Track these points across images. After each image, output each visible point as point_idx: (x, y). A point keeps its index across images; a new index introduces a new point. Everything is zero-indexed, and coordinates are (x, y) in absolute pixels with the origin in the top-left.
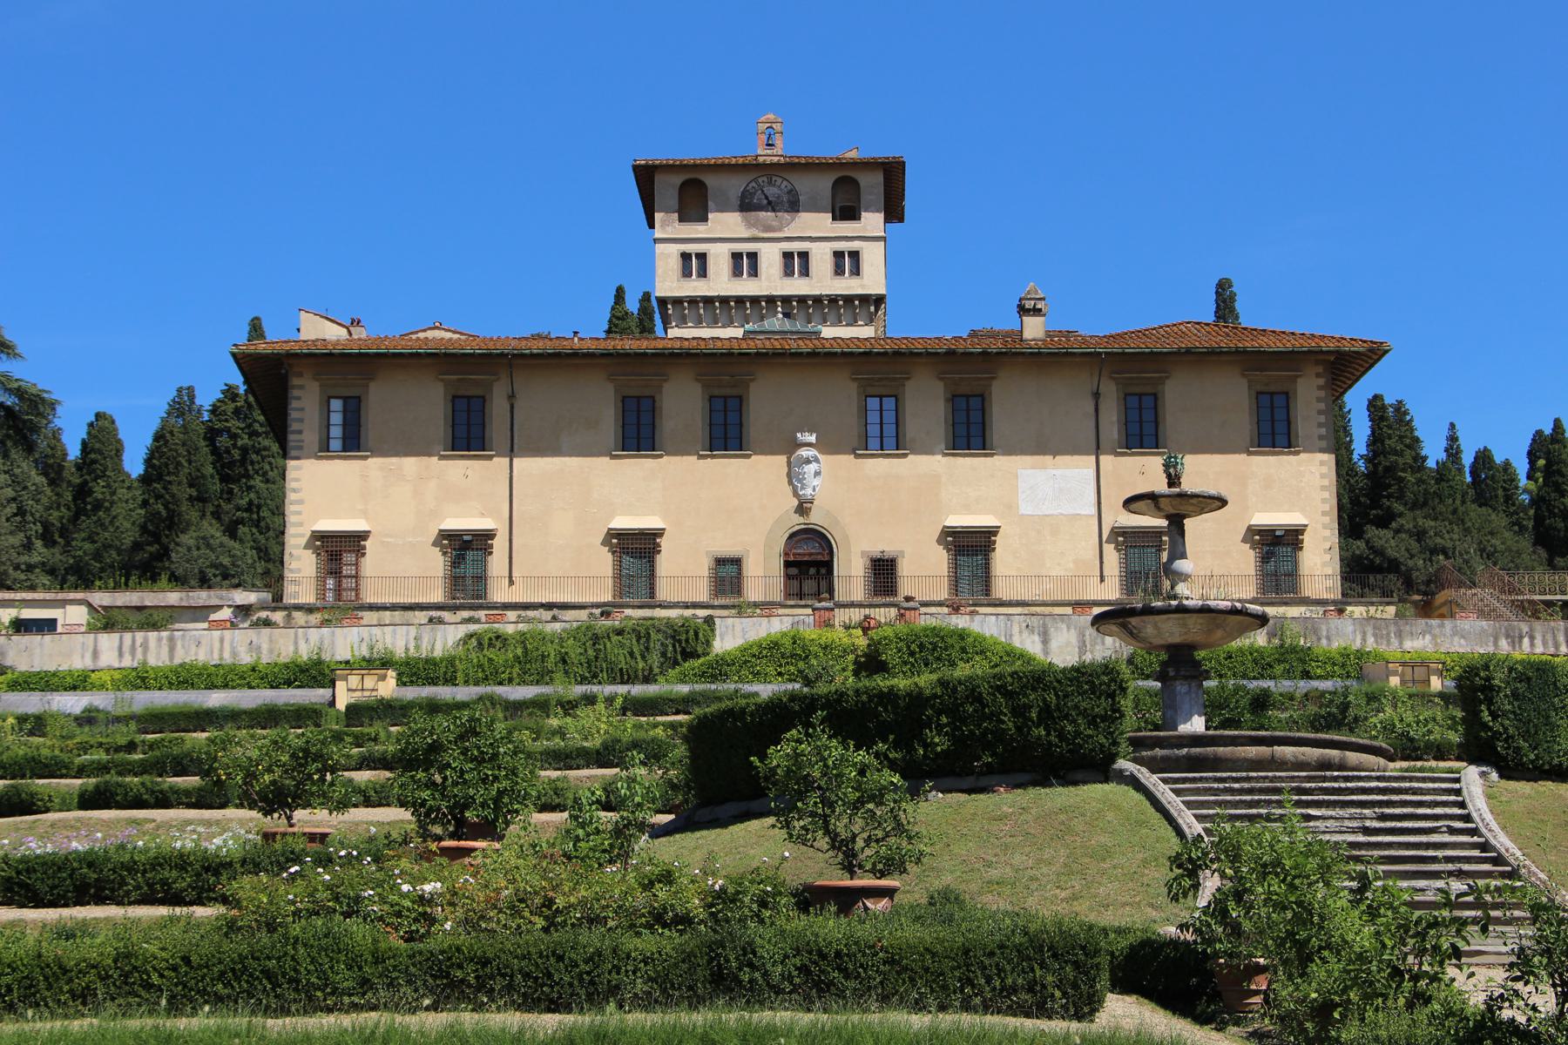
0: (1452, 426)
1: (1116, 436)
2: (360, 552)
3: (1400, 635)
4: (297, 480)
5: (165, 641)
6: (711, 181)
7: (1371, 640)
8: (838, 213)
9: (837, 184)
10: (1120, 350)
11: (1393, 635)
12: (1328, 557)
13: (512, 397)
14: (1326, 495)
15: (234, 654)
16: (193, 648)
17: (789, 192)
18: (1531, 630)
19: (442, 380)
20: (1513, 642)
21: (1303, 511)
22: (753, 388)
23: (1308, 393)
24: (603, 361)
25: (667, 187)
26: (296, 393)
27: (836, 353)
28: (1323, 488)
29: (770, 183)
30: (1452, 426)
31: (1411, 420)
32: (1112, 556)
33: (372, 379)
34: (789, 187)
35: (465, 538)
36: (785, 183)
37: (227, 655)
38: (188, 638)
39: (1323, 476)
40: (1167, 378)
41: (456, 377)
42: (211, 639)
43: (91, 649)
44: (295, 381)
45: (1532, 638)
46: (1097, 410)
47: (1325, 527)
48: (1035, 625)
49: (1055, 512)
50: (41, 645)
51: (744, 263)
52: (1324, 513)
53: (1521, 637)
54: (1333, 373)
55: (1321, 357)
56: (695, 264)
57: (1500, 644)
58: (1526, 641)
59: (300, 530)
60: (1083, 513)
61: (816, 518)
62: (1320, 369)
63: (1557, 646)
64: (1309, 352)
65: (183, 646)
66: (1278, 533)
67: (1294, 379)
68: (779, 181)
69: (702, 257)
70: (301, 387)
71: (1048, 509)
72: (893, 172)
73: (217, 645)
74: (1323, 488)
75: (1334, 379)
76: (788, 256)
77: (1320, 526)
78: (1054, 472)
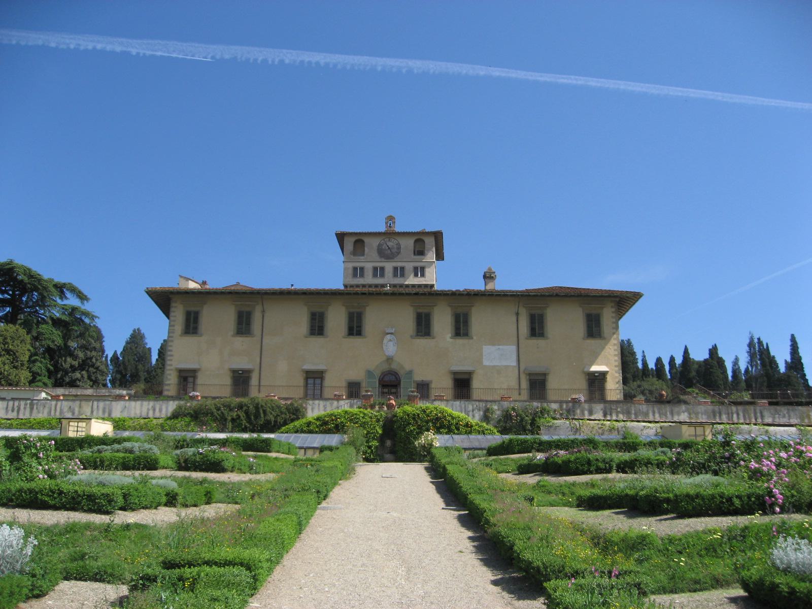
0: (643, 352)
1: (526, 331)
2: (195, 377)
3: (672, 414)
4: (171, 346)
5: (28, 406)
6: (367, 240)
7: (657, 415)
8: (416, 253)
9: (416, 241)
10: (527, 294)
11: (668, 413)
12: (617, 385)
13: (263, 311)
14: (616, 358)
15: (61, 412)
16: (42, 409)
17: (397, 245)
18: (737, 410)
19: (234, 304)
20: (729, 416)
21: (607, 365)
22: (368, 309)
23: (607, 314)
24: (303, 296)
25: (349, 243)
26: (172, 309)
28: (615, 355)
29: (389, 240)
30: (643, 352)
31: (632, 346)
32: (525, 384)
34: (397, 242)
35: (240, 372)
36: (395, 241)
37: (58, 413)
38: (39, 404)
39: (615, 350)
40: (548, 307)
41: (240, 303)
42: (51, 405)
44: (173, 304)
45: (738, 415)
46: (517, 321)
47: (616, 372)
48: (481, 406)
49: (499, 364)
51: (378, 272)
52: (616, 366)
53: (732, 414)
54: (619, 306)
55: (613, 299)
56: (358, 272)
57: (722, 417)
58: (735, 416)
60: (511, 364)
61: (394, 366)
62: (613, 304)
63: (750, 420)
64: (609, 296)
65: (37, 408)
66: (596, 375)
67: (602, 308)
68: (393, 240)
69: (362, 269)
70: (176, 307)
71: (496, 363)
72: (438, 236)
73: (53, 408)
74: (615, 355)
75: (619, 309)
76: (395, 269)
77: (614, 372)
78: (497, 347)
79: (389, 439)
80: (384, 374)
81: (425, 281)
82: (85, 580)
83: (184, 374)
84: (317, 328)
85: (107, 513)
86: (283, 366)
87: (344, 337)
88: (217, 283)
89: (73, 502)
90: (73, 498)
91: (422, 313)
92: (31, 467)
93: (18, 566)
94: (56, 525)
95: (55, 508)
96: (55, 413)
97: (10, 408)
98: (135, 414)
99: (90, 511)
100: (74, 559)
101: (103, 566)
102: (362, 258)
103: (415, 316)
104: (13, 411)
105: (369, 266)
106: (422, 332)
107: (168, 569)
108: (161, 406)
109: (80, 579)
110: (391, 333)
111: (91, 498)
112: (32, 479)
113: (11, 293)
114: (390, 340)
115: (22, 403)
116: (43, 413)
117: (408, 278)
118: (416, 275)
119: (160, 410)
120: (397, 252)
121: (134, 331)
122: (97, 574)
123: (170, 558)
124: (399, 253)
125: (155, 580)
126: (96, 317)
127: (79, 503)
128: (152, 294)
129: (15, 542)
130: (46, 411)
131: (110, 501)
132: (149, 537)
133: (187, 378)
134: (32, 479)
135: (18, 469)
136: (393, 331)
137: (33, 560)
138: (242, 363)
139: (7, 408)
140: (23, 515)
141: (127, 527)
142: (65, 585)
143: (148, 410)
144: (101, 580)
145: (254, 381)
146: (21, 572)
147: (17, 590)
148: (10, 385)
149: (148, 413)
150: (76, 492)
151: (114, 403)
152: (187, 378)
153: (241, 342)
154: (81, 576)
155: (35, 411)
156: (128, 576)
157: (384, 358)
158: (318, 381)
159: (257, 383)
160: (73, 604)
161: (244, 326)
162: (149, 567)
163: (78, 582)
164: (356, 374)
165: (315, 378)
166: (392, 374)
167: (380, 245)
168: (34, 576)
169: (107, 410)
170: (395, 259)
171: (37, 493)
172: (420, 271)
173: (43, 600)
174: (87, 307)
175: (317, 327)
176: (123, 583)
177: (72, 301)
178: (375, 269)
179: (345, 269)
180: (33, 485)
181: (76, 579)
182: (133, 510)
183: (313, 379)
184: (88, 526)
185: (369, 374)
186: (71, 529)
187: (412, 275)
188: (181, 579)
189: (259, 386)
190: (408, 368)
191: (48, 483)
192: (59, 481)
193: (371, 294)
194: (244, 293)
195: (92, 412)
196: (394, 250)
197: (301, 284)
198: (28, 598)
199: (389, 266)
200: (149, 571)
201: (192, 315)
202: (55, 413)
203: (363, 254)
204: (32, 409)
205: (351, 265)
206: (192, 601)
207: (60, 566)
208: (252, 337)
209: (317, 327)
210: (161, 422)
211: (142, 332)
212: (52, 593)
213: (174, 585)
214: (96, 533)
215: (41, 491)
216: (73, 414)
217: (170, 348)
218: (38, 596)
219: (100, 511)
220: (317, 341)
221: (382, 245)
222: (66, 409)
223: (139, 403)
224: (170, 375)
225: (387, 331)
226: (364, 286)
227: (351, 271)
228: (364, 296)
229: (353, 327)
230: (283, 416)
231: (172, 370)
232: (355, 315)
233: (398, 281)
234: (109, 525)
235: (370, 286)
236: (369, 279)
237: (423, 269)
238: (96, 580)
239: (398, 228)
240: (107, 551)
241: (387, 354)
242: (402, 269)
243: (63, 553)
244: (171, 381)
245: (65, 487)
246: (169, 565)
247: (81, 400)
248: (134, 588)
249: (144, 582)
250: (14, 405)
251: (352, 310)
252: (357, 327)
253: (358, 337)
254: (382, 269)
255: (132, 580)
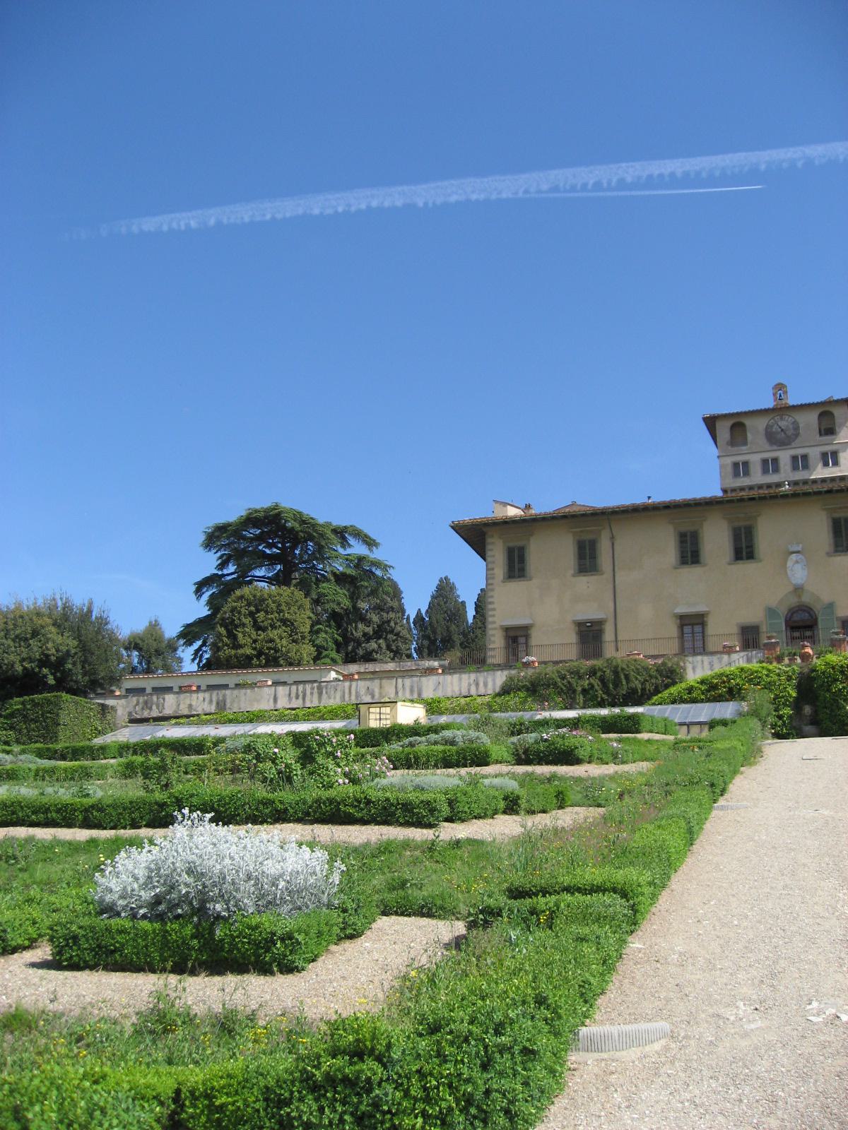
2: (527, 637)
4: (492, 597)
5: (316, 690)
6: (748, 422)
8: (823, 432)
9: (822, 415)
13: (612, 538)
15: (357, 696)
16: (333, 692)
17: (793, 423)
24: (667, 511)
25: (724, 430)
26: (489, 547)
27: (810, 493)
29: (782, 419)
33: (532, 535)
35: (588, 624)
37: (353, 697)
43: (272, 696)
44: (489, 540)
50: (245, 694)
56: (741, 469)
59: (494, 626)
61: (806, 599)
65: (326, 693)
68: (787, 417)
69: (746, 464)
70: (493, 543)
73: (347, 691)
76: (794, 458)
79: (808, 704)
80: (792, 612)
81: (840, 471)
82: (409, 915)
83: (512, 634)
84: (689, 554)
85: (430, 826)
86: (646, 612)
87: (730, 564)
88: (544, 505)
89: (385, 814)
90: (385, 808)
91: (840, 518)
92: (327, 770)
93: (325, 899)
94: (367, 844)
95: (363, 822)
96: (350, 697)
97: (293, 695)
98: (453, 691)
99: (408, 824)
100: (392, 889)
101: (429, 896)
102: (744, 448)
103: (831, 524)
104: (297, 697)
105: (755, 459)
106: (842, 546)
107: (515, 898)
108: (486, 679)
109: (402, 914)
110: (798, 552)
111: (407, 807)
112: (330, 786)
113: (280, 545)
114: (797, 562)
115: (308, 687)
116: (335, 698)
117: (814, 470)
118: (826, 464)
119: (486, 685)
120: (794, 435)
121: (441, 580)
122: (423, 907)
123: (517, 884)
124: (797, 435)
125: (499, 914)
126: (390, 567)
127: (393, 814)
128: (460, 529)
129: (318, 868)
130: (338, 695)
131: (432, 811)
132: (486, 856)
133: (517, 638)
134: (330, 786)
135: (311, 773)
136: (799, 548)
137: (341, 891)
138: (590, 613)
139: (290, 695)
140: (324, 832)
141: (457, 844)
142: (383, 922)
143: (470, 685)
144: (430, 915)
145: (608, 636)
146: (329, 906)
147: (326, 929)
148: (291, 664)
149: (469, 690)
150: (387, 800)
151: (424, 679)
152: (517, 638)
153: (585, 583)
154: (403, 910)
155: (324, 696)
156: (463, 909)
157: (791, 588)
158: (698, 629)
159: (614, 639)
160: (396, 947)
161: (587, 560)
162: (490, 896)
163: (401, 919)
164: (754, 615)
165: (693, 625)
166: (804, 611)
167: (768, 428)
168: (345, 911)
169: (416, 689)
170: (793, 445)
171: (339, 804)
172: (831, 458)
173: (359, 941)
174: (376, 554)
175: (690, 553)
176: (458, 919)
177: (357, 549)
178: (765, 462)
179: (722, 467)
180: (331, 793)
181: (396, 914)
182: (463, 821)
183: (690, 627)
184: (406, 844)
185: (771, 612)
186: (386, 848)
187: (820, 465)
188: (533, 912)
189: (616, 641)
190: (826, 598)
191: (351, 790)
192: (364, 787)
193: (763, 498)
194: (583, 515)
195: (397, 693)
196: (790, 433)
197: (659, 497)
198: (340, 939)
199: (784, 456)
200: (491, 902)
201: (516, 552)
202: (350, 697)
203: (745, 443)
204: (320, 694)
205: (729, 461)
206: (551, 942)
207: (376, 897)
208: (602, 574)
209: (690, 553)
210: (487, 700)
211: (451, 581)
212: (368, 933)
213: (525, 920)
214: (417, 853)
215: (343, 801)
216: (373, 697)
217: (490, 600)
218: (351, 937)
219: (420, 824)
220: (691, 574)
221: (772, 426)
222: (363, 691)
223: (456, 676)
224: (493, 635)
225: (792, 549)
226: (751, 488)
227: (730, 469)
228: (752, 503)
229: (742, 548)
230: (653, 681)
231: (495, 629)
232: (743, 530)
233: (800, 475)
234: (433, 843)
235: (760, 487)
236: (757, 477)
237: (835, 454)
238: (423, 915)
239: (792, 400)
240: (434, 877)
241: (794, 582)
242: (805, 457)
243: (378, 880)
244: (496, 643)
245: (374, 795)
246: (517, 893)
247: (381, 679)
248: (472, 925)
249: (485, 918)
250: (297, 690)
251: (737, 524)
252: (747, 547)
253: (749, 561)
254: (775, 461)
255: (470, 914)
